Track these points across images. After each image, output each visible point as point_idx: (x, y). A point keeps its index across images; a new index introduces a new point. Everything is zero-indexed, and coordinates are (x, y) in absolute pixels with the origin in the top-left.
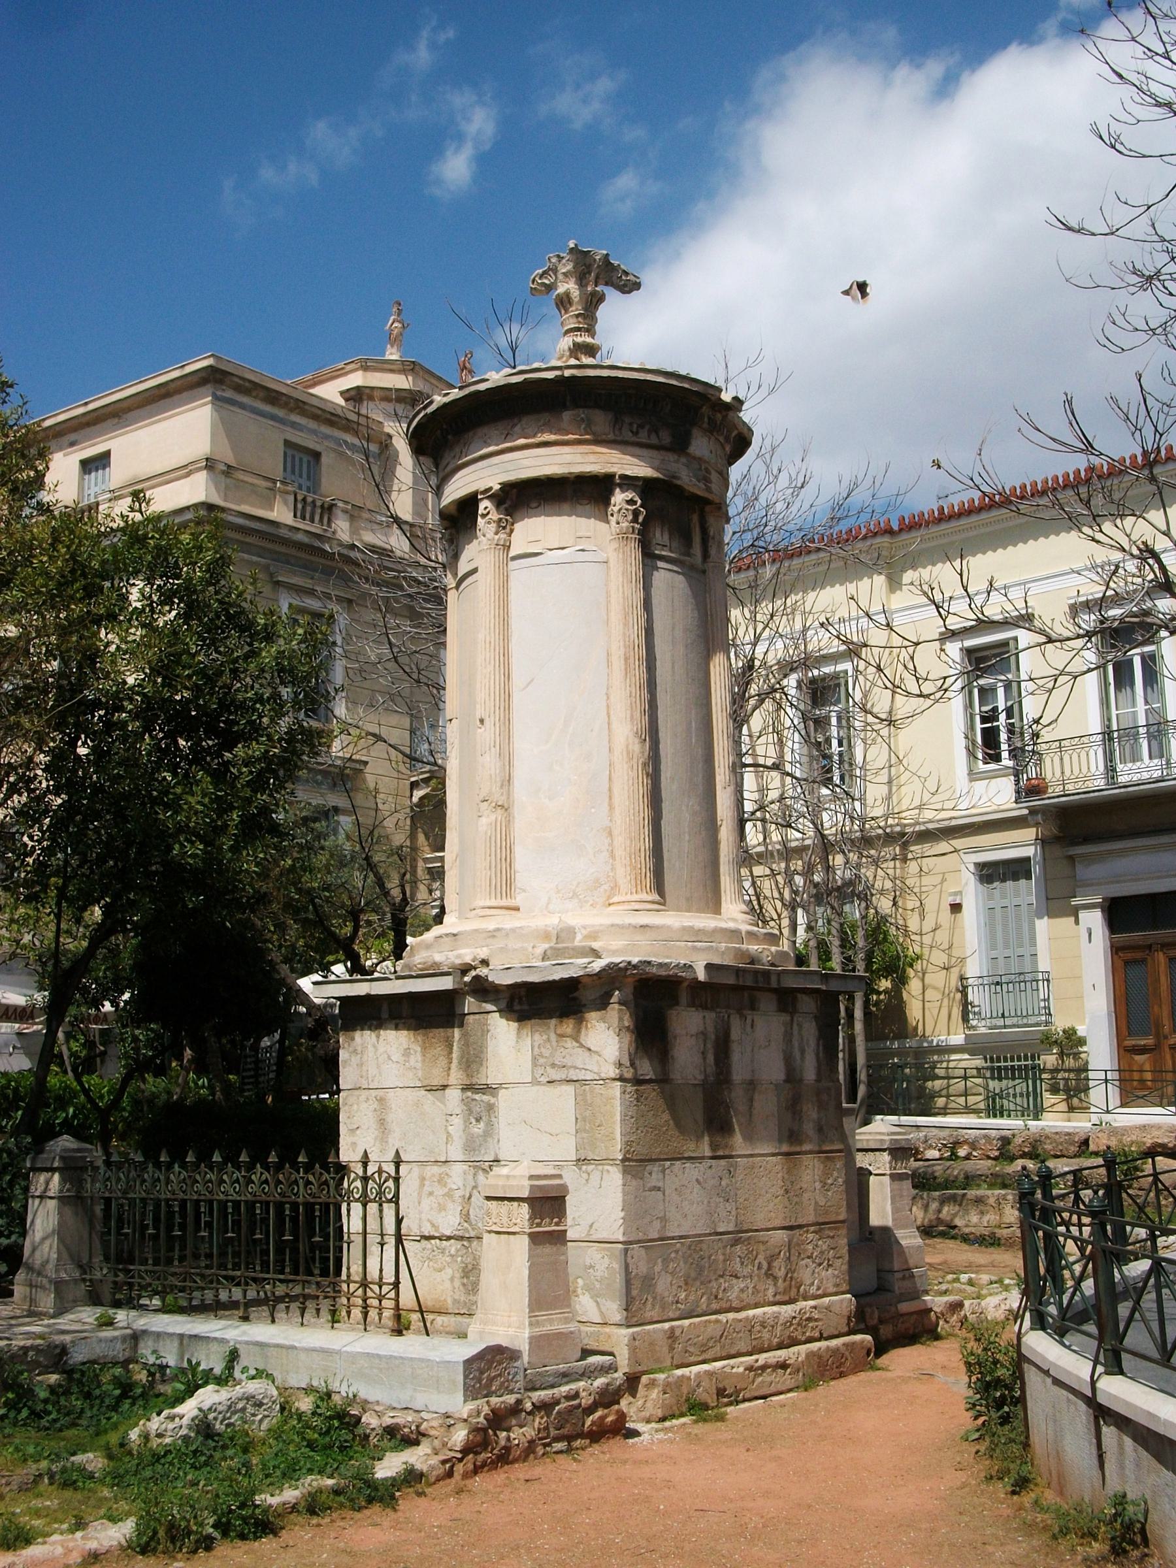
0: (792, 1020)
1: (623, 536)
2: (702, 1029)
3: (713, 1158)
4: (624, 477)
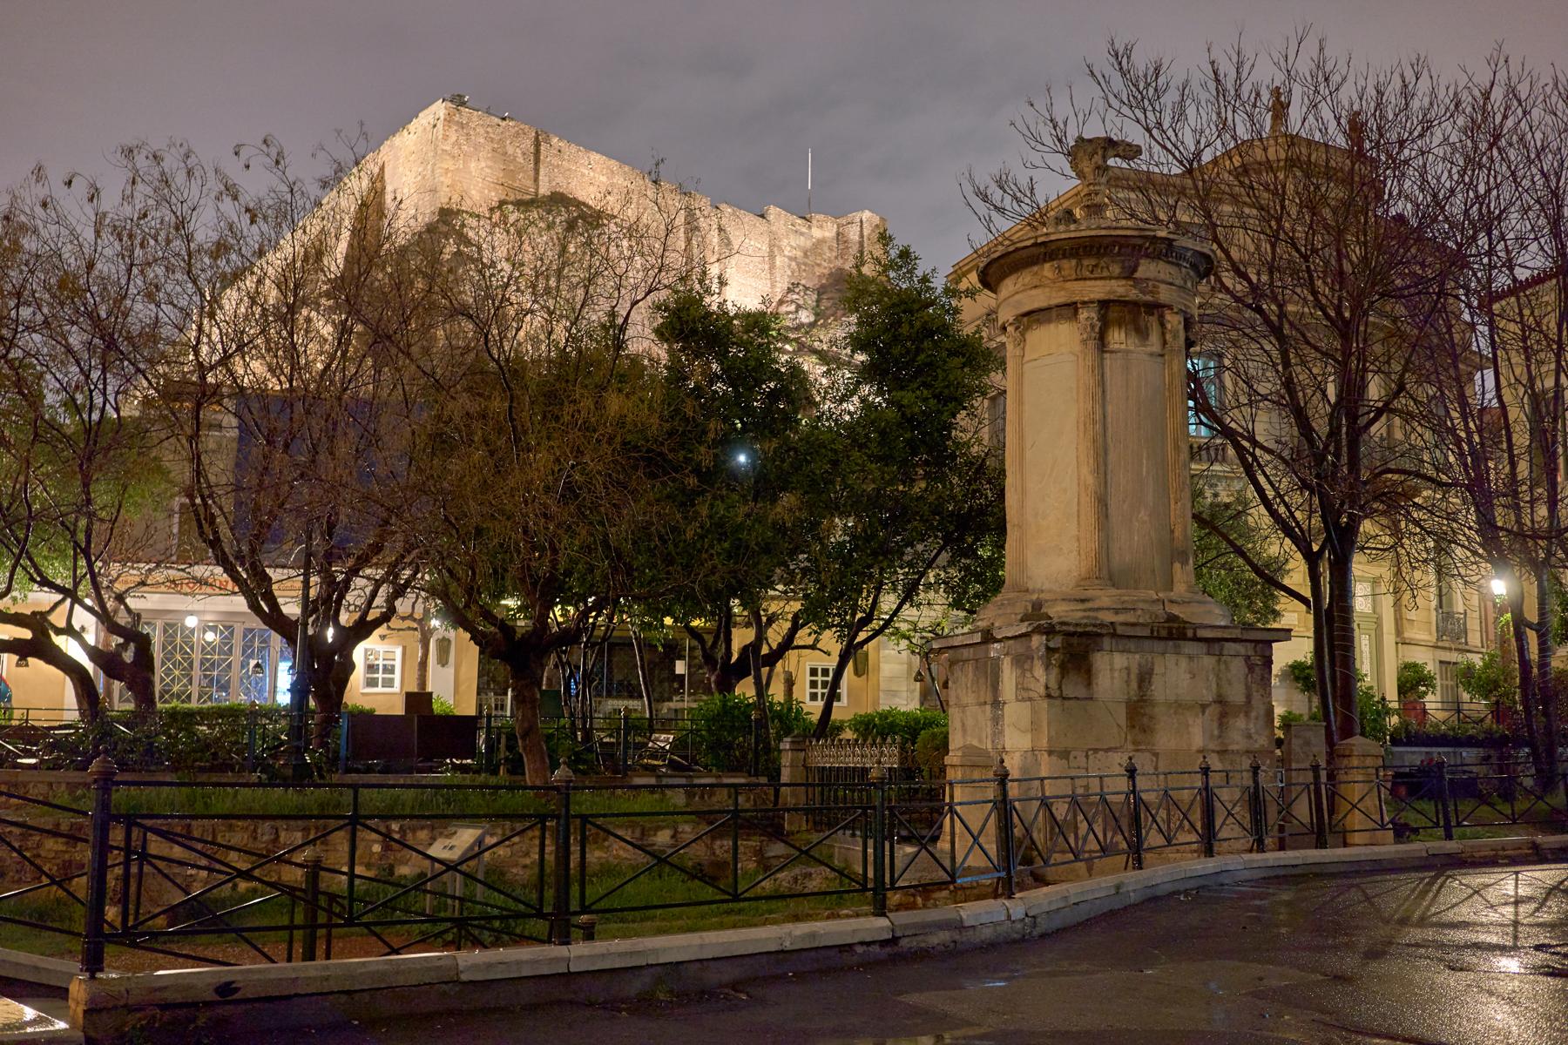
0: (1219, 660)
1: (1084, 342)
2: (1125, 664)
3: (1137, 750)
4: (1084, 303)
